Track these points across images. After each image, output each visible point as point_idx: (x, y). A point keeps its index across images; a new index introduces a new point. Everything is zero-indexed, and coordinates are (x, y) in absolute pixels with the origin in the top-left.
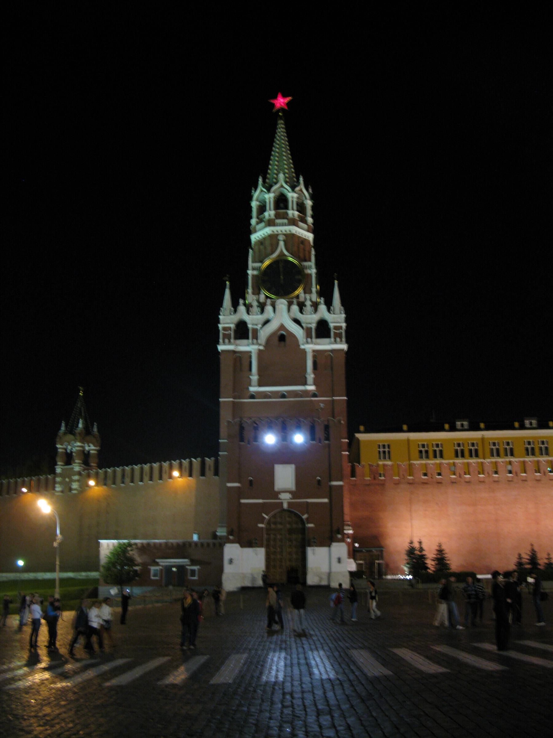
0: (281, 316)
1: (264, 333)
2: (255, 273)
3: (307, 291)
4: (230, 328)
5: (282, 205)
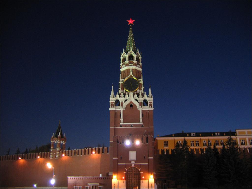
0: (131, 98)
1: (125, 104)
2: (122, 82)
4: (113, 102)
5: (131, 59)
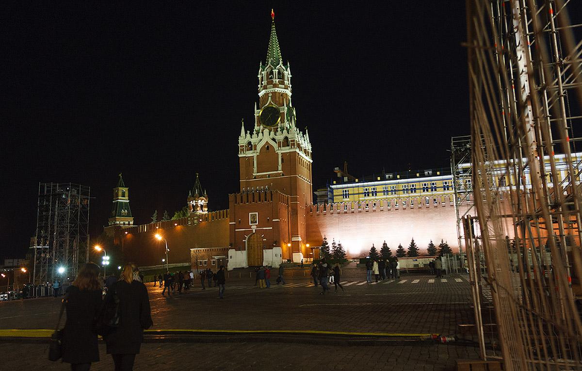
3: (282, 121)
